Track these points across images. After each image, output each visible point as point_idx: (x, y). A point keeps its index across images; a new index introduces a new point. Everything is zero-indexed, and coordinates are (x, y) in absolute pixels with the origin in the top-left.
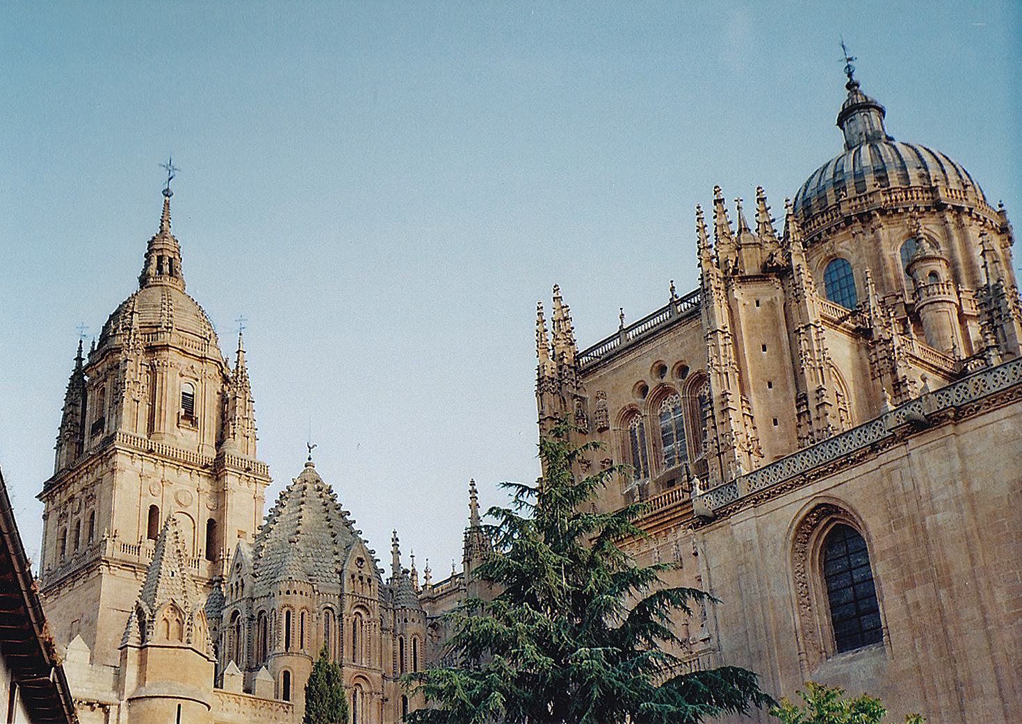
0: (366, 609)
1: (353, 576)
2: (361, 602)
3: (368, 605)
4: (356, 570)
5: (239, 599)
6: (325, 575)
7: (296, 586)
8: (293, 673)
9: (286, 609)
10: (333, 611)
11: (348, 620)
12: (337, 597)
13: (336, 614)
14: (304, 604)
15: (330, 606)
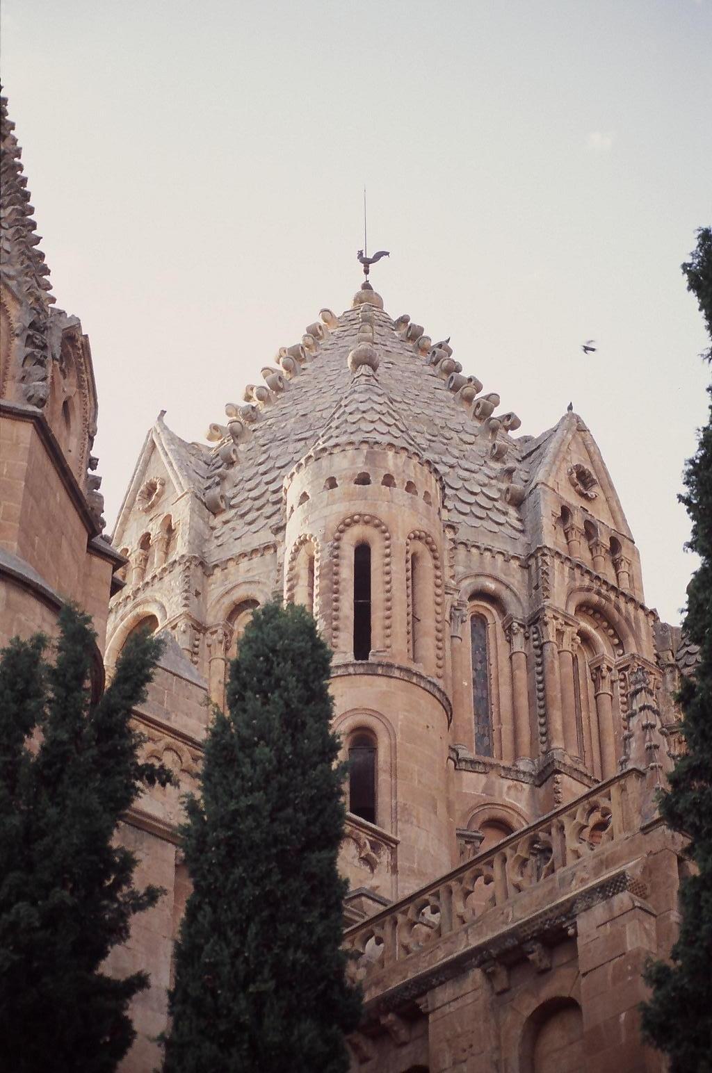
0: (612, 624)
1: (565, 513)
2: (599, 593)
3: (618, 609)
4: (573, 500)
5: (148, 578)
6: (472, 499)
7: (392, 462)
8: (391, 734)
9: (356, 532)
10: (502, 610)
11: (560, 633)
12: (515, 564)
13: (518, 611)
14: (422, 524)
15: (491, 586)
